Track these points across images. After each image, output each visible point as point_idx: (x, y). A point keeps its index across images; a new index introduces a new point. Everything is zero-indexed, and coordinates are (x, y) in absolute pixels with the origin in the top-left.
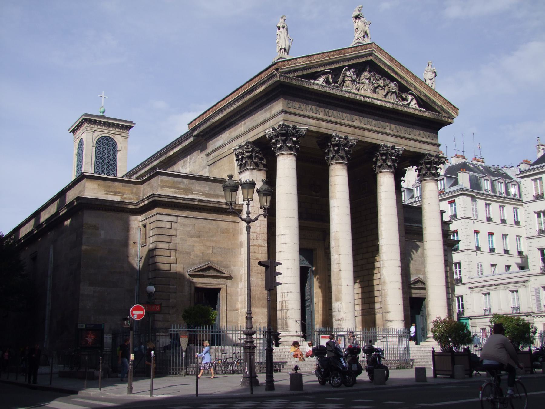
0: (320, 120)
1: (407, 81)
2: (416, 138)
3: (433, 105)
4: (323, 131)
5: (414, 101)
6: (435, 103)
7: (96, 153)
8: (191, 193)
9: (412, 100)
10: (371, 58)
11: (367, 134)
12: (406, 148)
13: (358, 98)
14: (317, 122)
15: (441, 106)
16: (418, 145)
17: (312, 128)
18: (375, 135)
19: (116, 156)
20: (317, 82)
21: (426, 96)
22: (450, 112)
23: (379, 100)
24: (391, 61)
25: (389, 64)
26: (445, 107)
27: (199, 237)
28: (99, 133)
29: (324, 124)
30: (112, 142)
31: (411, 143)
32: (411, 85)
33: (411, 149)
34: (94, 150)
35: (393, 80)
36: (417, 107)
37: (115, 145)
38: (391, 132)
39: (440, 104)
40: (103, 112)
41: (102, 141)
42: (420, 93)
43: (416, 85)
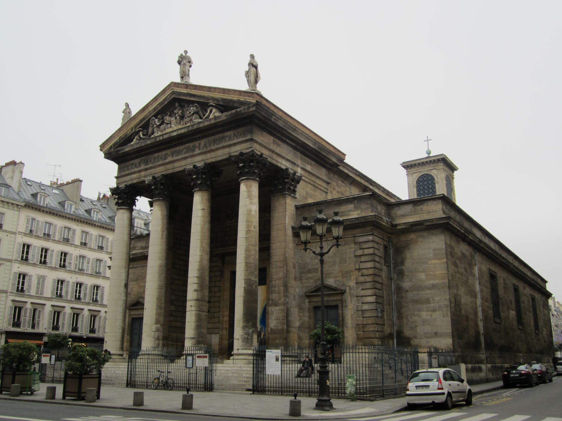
0: (140, 171)
1: (204, 97)
2: (229, 143)
3: (231, 104)
4: (143, 179)
5: (214, 110)
6: (232, 101)
7: (418, 191)
8: (135, 250)
9: (211, 111)
10: (174, 96)
11: (176, 164)
12: (214, 160)
13: (165, 137)
14: (138, 174)
15: (238, 100)
16: (227, 151)
17: (135, 181)
18: (183, 163)
19: (435, 188)
20: (132, 143)
21: (223, 100)
22: (248, 100)
23: (175, 131)
24: (186, 88)
25: (185, 92)
26: (241, 100)
27: (136, 280)
28: (417, 174)
29: (143, 173)
30: (430, 178)
31: (220, 152)
32: (208, 98)
33: (220, 159)
34: (415, 190)
35: (193, 102)
36: (217, 114)
37: (433, 179)
38: (200, 151)
39: (236, 99)
40: (429, 153)
41: (430, 178)
42: (218, 100)
43: (211, 95)
